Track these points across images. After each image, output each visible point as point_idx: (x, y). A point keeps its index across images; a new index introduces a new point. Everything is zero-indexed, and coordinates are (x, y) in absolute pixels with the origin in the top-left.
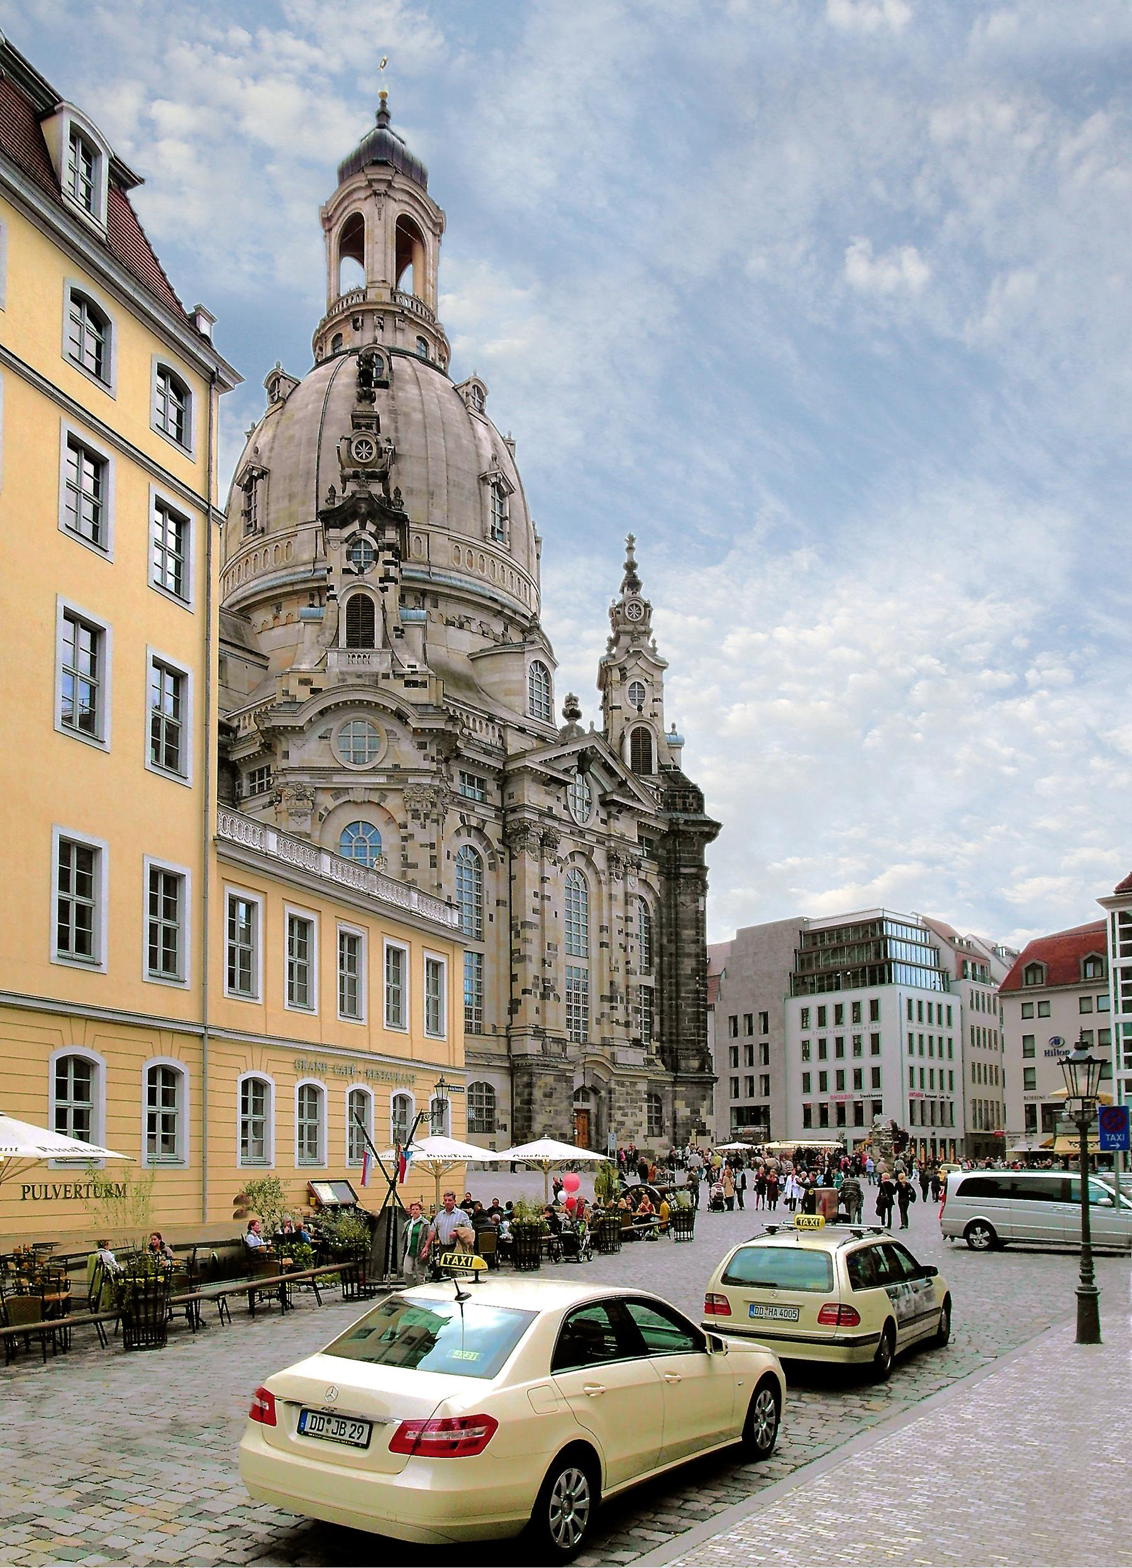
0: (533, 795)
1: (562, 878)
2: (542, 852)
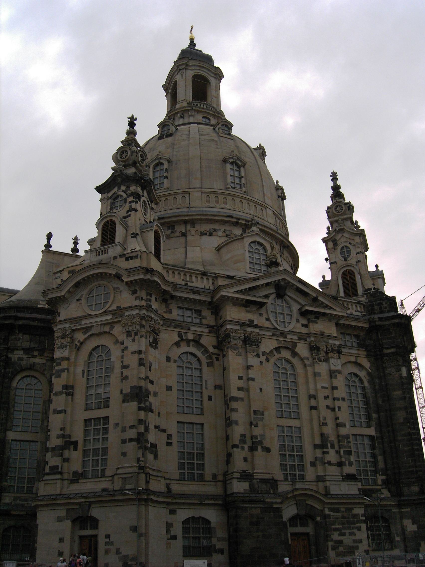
0: (232, 313)
2: (246, 349)
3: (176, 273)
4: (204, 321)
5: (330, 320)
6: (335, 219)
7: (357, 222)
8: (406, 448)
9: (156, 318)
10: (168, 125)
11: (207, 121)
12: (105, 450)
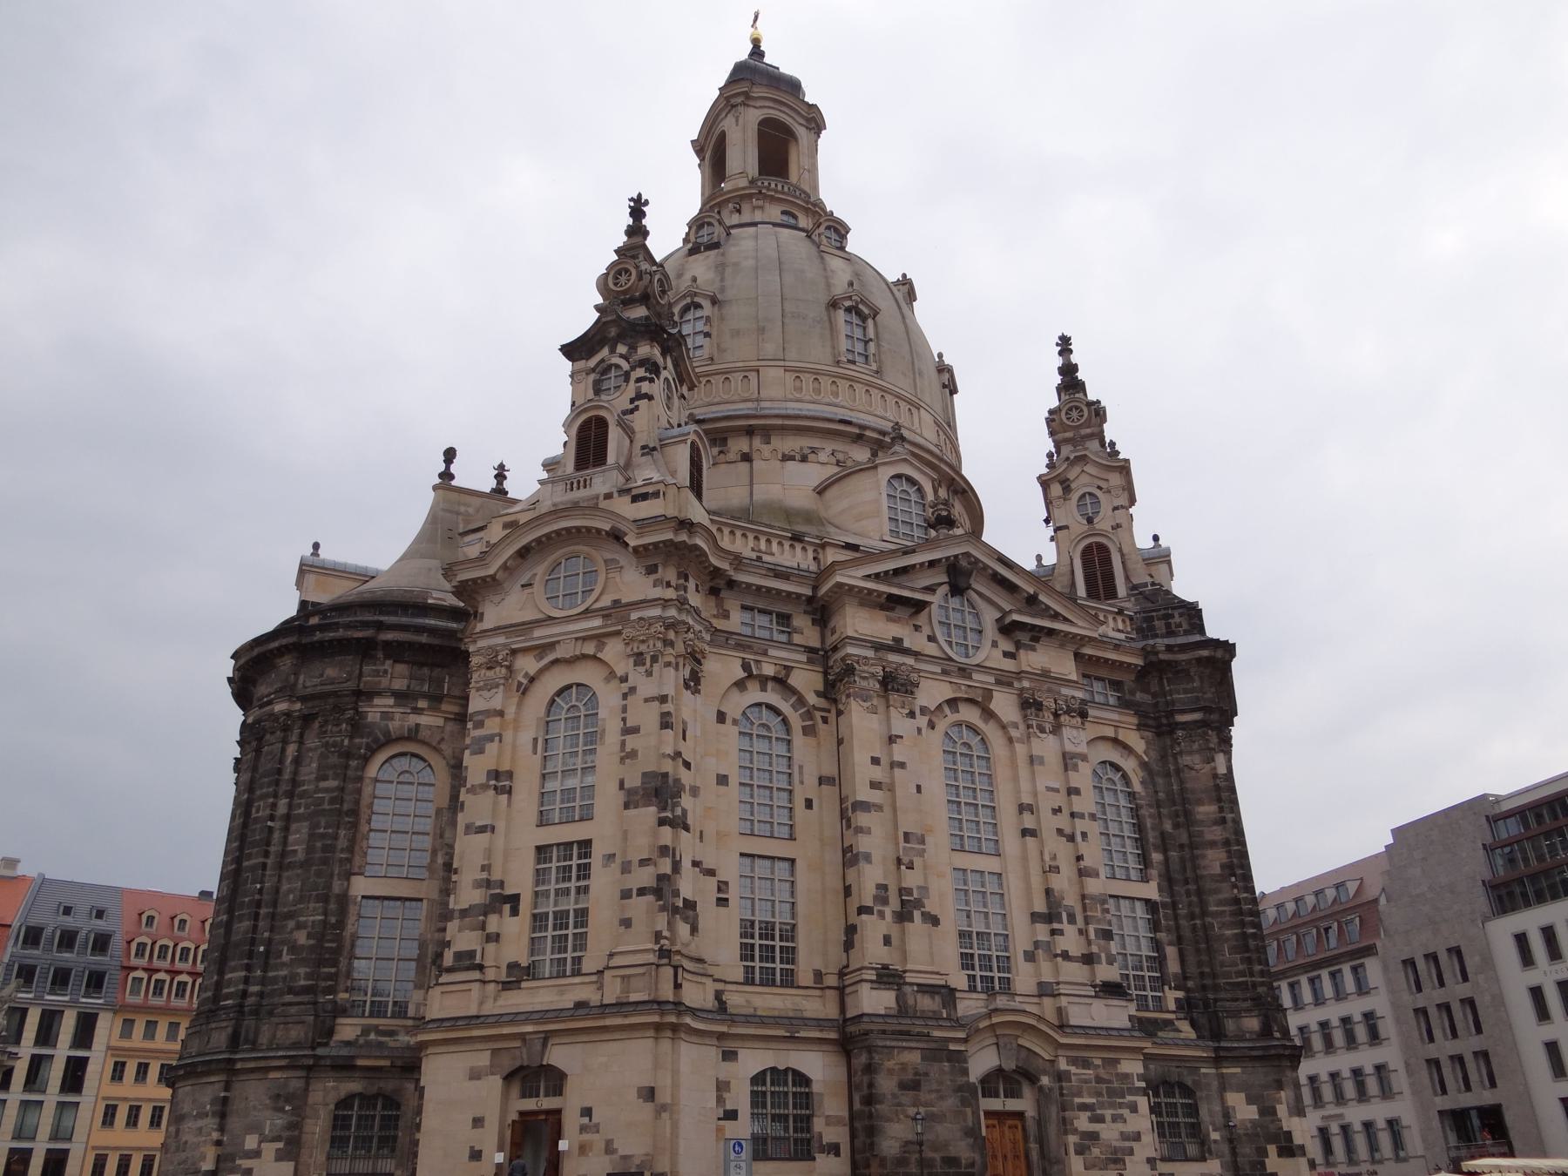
0: (858, 623)
1: (935, 739)
2: (887, 701)
3: (738, 533)
4: (797, 639)
5: (1062, 646)
6: (1069, 435)
7: (1112, 444)
8: (1228, 932)
9: (698, 627)
10: (710, 224)
11: (792, 221)
12: (582, 914)
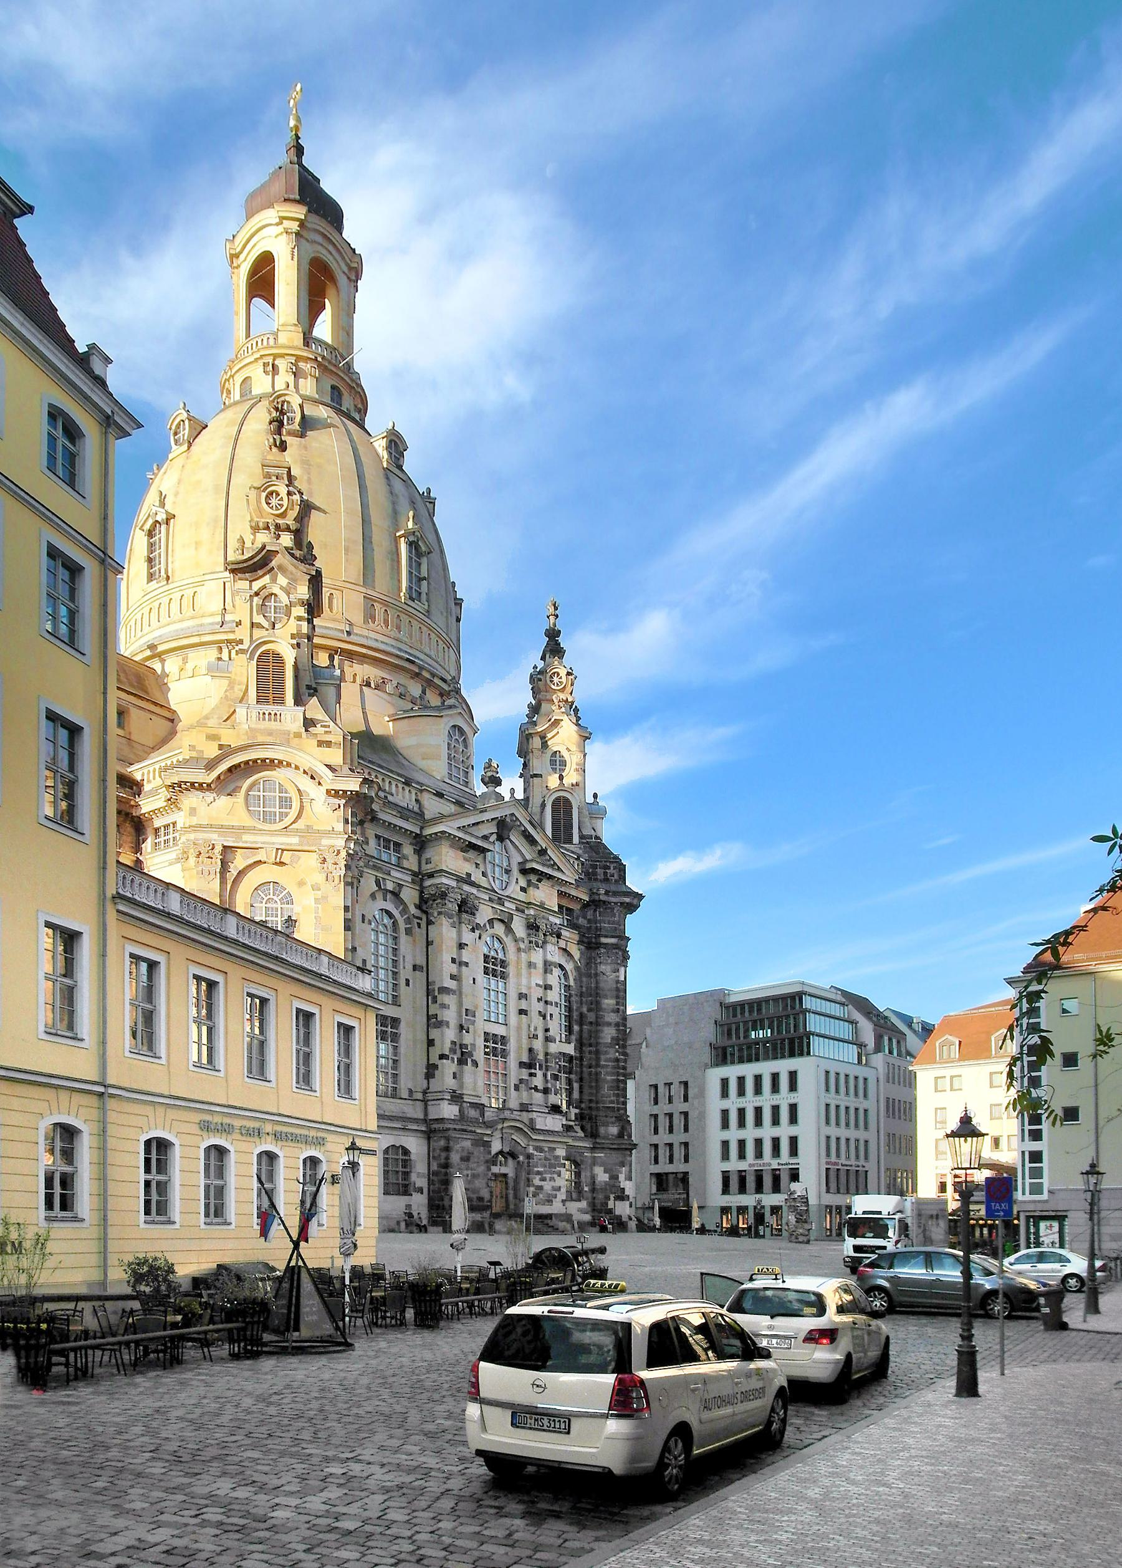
2: (460, 918)
8: (609, 1078)
